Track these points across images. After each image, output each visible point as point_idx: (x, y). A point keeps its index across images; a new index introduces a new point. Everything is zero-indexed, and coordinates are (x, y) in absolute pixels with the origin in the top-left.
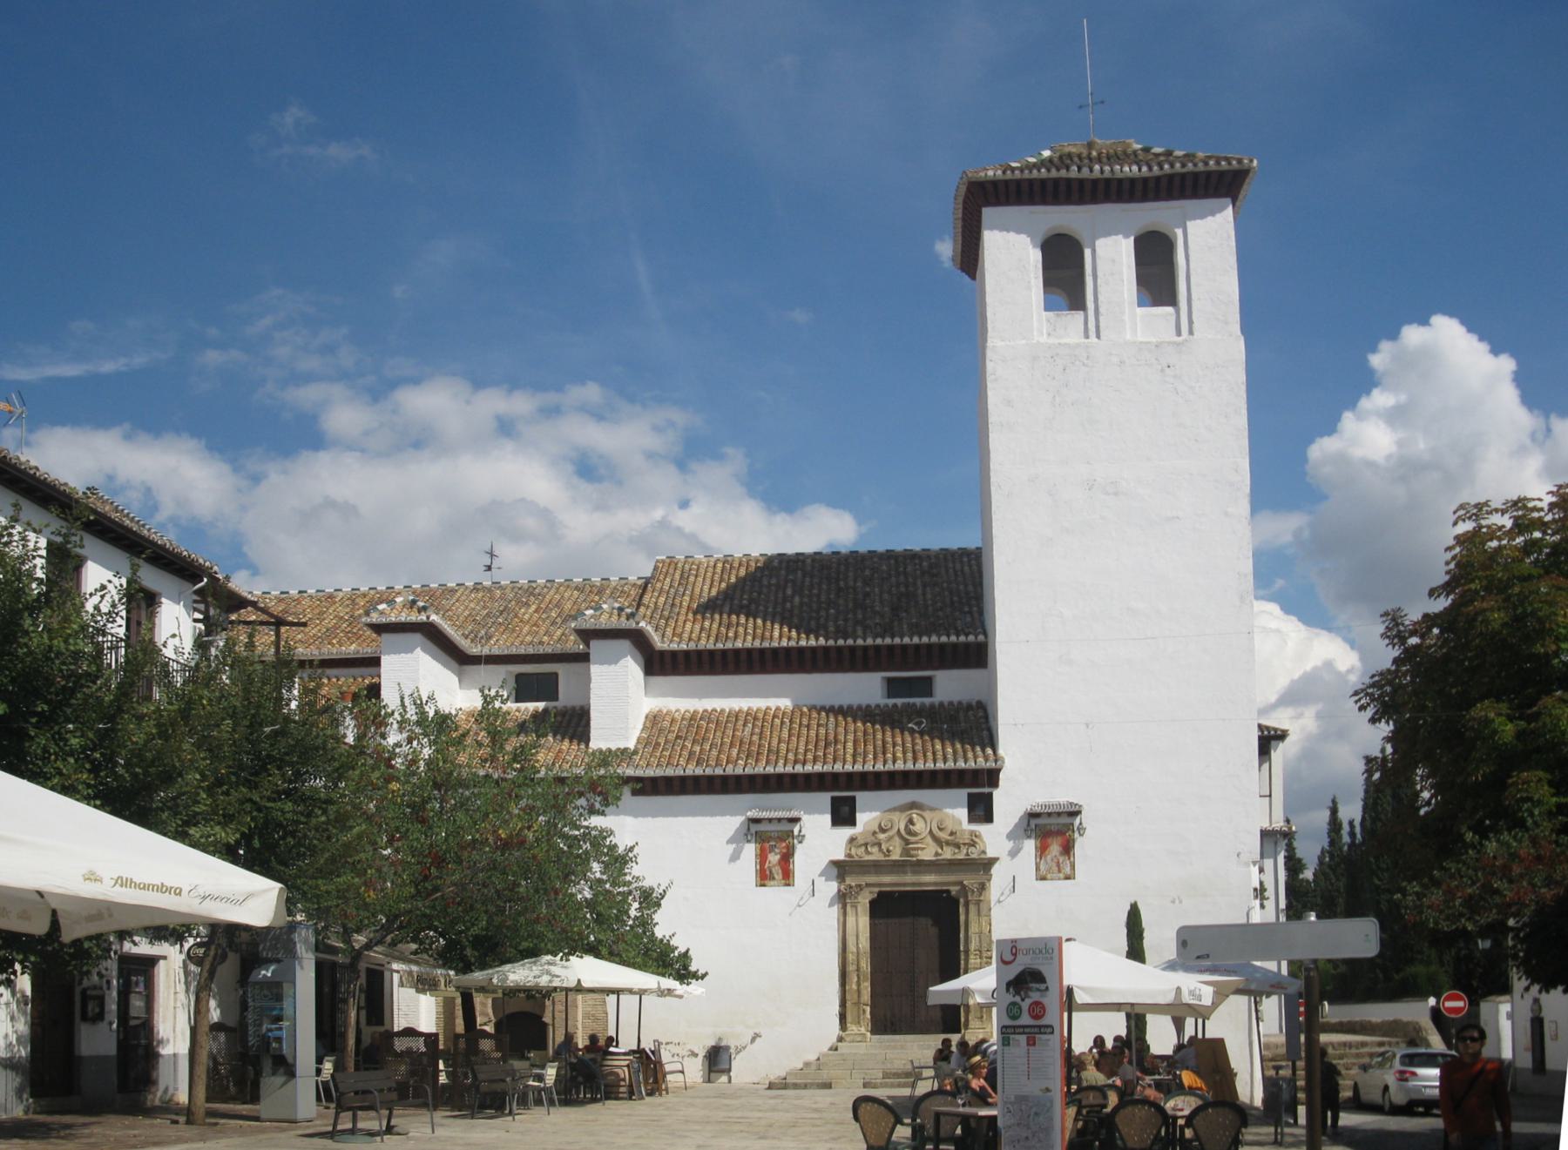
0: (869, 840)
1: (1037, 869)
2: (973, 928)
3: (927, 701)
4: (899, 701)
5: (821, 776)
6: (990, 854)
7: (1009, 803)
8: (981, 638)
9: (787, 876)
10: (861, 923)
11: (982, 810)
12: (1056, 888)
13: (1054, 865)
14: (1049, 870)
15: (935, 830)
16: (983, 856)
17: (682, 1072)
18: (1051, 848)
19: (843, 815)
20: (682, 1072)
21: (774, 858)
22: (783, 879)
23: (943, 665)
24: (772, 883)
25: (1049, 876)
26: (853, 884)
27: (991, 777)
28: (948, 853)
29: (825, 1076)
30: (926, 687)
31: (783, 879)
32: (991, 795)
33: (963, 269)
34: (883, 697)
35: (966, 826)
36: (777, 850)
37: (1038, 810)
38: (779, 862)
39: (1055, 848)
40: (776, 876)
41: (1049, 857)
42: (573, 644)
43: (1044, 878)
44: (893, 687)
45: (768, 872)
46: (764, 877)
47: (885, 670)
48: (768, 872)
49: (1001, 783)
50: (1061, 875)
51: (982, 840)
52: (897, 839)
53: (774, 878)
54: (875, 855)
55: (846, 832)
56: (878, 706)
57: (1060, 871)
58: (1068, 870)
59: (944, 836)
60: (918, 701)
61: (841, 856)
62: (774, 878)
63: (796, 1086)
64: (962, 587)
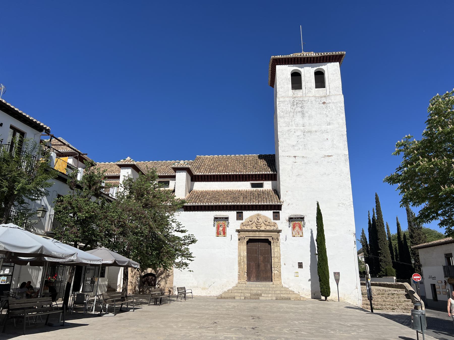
0: (246, 224)
1: (292, 233)
2: (276, 250)
3: (261, 189)
4: (255, 189)
5: (234, 206)
6: (279, 229)
7: (284, 214)
8: (275, 173)
9: (224, 233)
10: (244, 247)
11: (276, 216)
12: (298, 239)
13: (297, 233)
14: (296, 234)
15: (264, 222)
16: (277, 229)
17: (191, 293)
18: (296, 227)
19: (240, 217)
20: (191, 293)
21: (221, 229)
22: (223, 234)
23: (266, 180)
24: (220, 236)
25: (296, 236)
26: (242, 236)
27: (279, 207)
28: (268, 228)
29: (232, 295)
30: (261, 186)
31: (223, 234)
32: (279, 212)
33: (271, 85)
34: (250, 188)
35: (272, 221)
36: (222, 227)
37: (291, 217)
38: (222, 229)
39: (297, 228)
40: (221, 234)
41: (295, 230)
42: (172, 173)
43: (294, 236)
44: (253, 186)
45: (219, 233)
46: (218, 234)
47: (252, 181)
48: (219, 233)
49: (282, 209)
50: (299, 236)
51: (277, 225)
52: (254, 223)
53: (221, 234)
54: (249, 228)
55: (241, 222)
56: (249, 190)
57: (299, 235)
58: (301, 234)
59: (267, 223)
60: (259, 189)
61: (239, 228)
62: (221, 234)
63: (224, 298)
64: (271, 159)
